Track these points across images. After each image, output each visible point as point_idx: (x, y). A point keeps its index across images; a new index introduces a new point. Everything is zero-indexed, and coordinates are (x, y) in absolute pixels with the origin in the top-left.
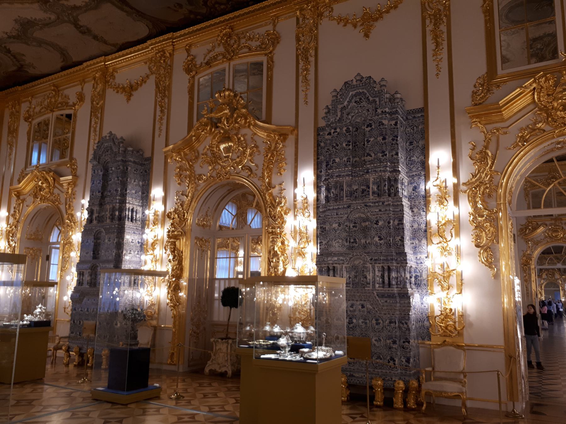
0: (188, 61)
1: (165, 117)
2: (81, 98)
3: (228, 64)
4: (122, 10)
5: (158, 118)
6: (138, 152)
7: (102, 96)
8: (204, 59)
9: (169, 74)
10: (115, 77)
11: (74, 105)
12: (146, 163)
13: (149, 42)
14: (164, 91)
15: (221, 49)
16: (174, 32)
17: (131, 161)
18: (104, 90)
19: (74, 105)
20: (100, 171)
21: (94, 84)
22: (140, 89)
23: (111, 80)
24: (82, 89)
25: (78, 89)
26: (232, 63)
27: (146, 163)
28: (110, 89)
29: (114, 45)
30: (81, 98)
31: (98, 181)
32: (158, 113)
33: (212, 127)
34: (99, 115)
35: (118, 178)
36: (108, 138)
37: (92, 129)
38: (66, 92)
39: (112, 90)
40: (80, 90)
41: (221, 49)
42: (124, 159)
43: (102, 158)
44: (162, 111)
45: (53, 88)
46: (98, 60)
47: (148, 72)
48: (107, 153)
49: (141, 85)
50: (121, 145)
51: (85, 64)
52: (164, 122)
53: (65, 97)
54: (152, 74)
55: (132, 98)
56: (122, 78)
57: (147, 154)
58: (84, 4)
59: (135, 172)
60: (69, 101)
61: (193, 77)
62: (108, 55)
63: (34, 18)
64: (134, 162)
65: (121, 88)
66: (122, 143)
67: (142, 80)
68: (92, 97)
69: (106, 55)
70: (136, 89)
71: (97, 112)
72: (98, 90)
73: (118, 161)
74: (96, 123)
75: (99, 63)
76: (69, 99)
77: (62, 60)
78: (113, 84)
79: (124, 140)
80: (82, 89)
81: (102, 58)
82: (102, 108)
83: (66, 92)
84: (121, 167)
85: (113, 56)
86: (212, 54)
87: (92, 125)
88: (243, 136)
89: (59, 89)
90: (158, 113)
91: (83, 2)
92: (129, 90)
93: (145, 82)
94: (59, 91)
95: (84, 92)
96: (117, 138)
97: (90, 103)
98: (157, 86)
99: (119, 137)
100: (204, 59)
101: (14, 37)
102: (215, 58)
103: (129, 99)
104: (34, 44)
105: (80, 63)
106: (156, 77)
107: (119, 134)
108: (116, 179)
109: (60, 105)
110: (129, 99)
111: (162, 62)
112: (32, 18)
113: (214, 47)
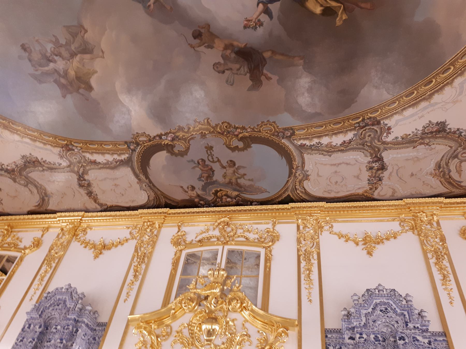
0: (178, 236)
1: (138, 283)
2: (37, 244)
3: (221, 247)
4: (137, 176)
5: (128, 281)
6: (94, 313)
7: (65, 247)
8: (196, 237)
9: (153, 243)
10: (86, 233)
11: (25, 248)
12: (97, 328)
13: (140, 211)
14: (142, 258)
15: (217, 233)
16: (170, 209)
17: (84, 322)
18: (69, 242)
19: (25, 248)
20: (37, 327)
21: (59, 235)
22: (113, 249)
23: (80, 235)
24: (42, 236)
25: (38, 234)
26: (227, 247)
27: (97, 328)
28: (76, 243)
29: (101, 205)
30: (37, 244)
31: (31, 340)
32: (131, 277)
33: (197, 304)
34: (54, 265)
35: (61, 340)
36: (63, 290)
37: (38, 277)
38: (20, 235)
39: (80, 243)
40: (39, 236)
41: (217, 233)
42: (77, 319)
43: (47, 311)
44: (135, 276)
45: (6, 227)
46: (76, 214)
47: (129, 236)
48: (56, 307)
49: (116, 246)
50: (80, 301)
51: (59, 214)
52: (136, 287)
53: (18, 239)
54: (133, 239)
55: (101, 256)
56: (94, 235)
57: (103, 319)
58: (105, 161)
59: (83, 337)
60: (20, 243)
61: (181, 251)
62: (89, 212)
63: (44, 160)
64: (87, 325)
65: (92, 244)
66: (82, 299)
67: (120, 242)
68: (52, 245)
69: (87, 211)
70: (109, 249)
71: (52, 261)
72: (62, 241)
73: (70, 320)
74: (46, 272)
75: (75, 217)
76: (21, 242)
77: (37, 204)
78: (82, 239)
79: (85, 296)
80: (42, 236)
81: (81, 213)
82: (60, 259)
83: (20, 235)
84: (71, 327)
85: (95, 214)
86: (204, 235)
87: (40, 273)
88: (233, 321)
89: (13, 230)
90: (131, 277)
91: (106, 160)
92: (101, 248)
93: (122, 244)
94: (11, 232)
95: (43, 239)
96: (77, 292)
97: (48, 250)
98: (136, 251)
99: (79, 291)
100: (196, 237)
101: (7, 171)
102: (209, 239)
103: (96, 257)
104: (22, 182)
105: (54, 212)
106: (137, 243)
107: (81, 288)
108: (59, 341)
109: (7, 245)
110: (96, 257)
111: (148, 230)
112: (42, 159)
113: (208, 230)
